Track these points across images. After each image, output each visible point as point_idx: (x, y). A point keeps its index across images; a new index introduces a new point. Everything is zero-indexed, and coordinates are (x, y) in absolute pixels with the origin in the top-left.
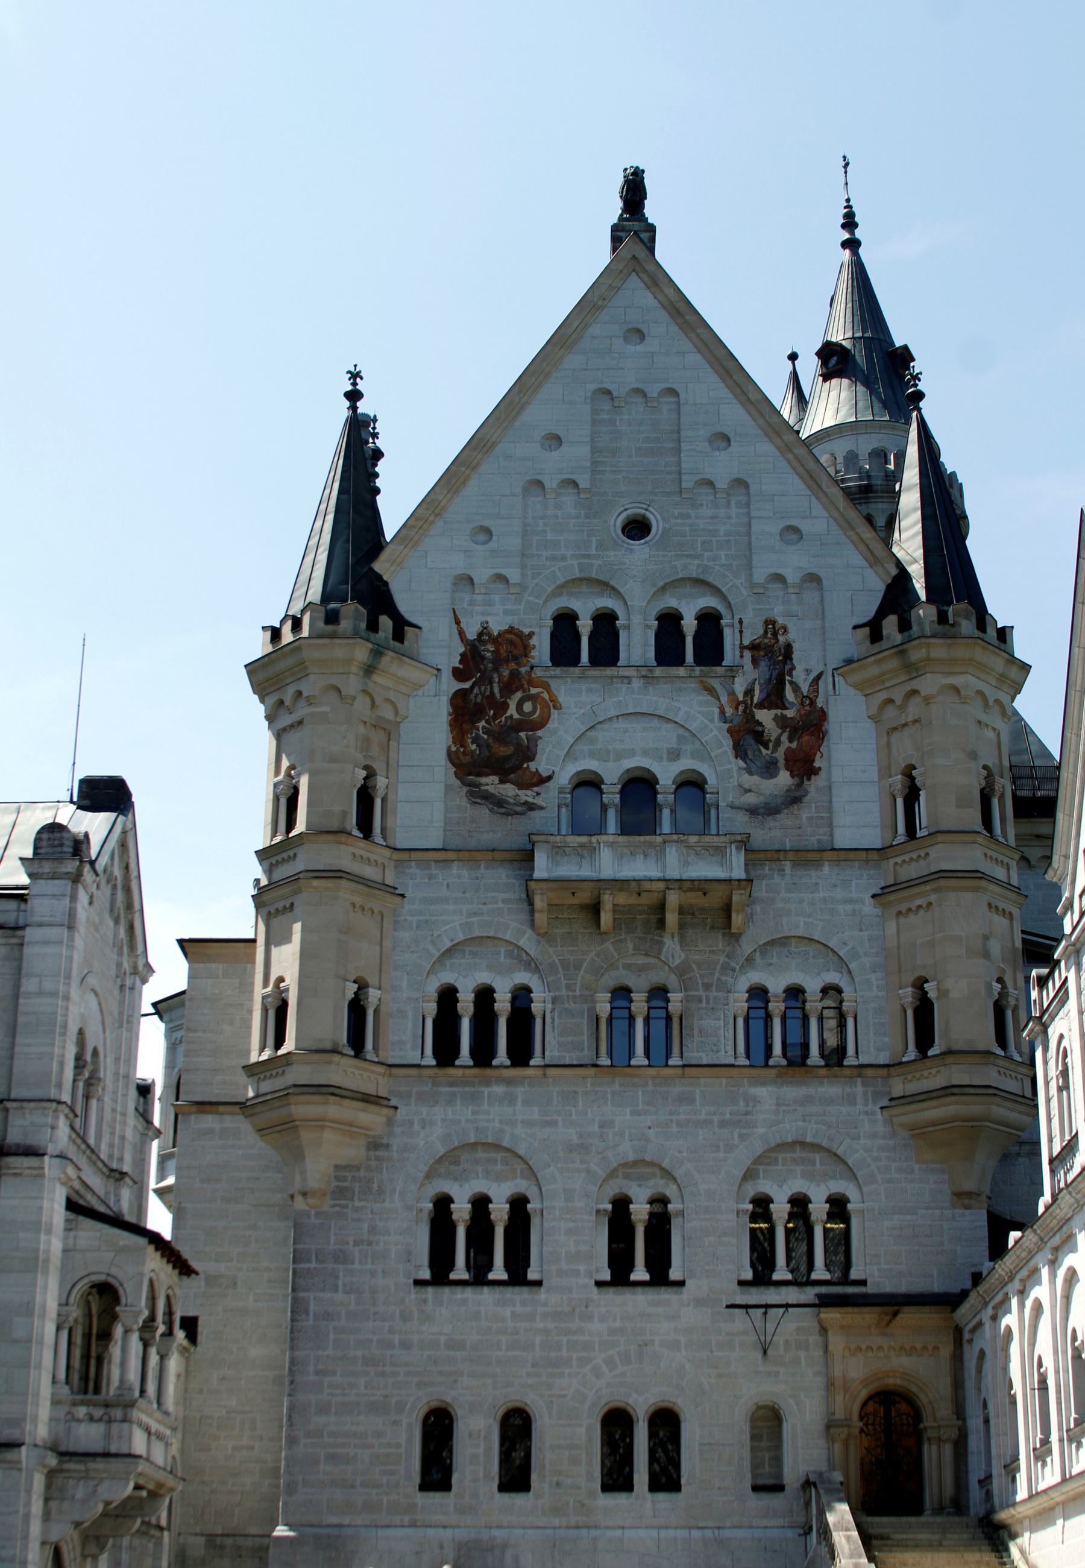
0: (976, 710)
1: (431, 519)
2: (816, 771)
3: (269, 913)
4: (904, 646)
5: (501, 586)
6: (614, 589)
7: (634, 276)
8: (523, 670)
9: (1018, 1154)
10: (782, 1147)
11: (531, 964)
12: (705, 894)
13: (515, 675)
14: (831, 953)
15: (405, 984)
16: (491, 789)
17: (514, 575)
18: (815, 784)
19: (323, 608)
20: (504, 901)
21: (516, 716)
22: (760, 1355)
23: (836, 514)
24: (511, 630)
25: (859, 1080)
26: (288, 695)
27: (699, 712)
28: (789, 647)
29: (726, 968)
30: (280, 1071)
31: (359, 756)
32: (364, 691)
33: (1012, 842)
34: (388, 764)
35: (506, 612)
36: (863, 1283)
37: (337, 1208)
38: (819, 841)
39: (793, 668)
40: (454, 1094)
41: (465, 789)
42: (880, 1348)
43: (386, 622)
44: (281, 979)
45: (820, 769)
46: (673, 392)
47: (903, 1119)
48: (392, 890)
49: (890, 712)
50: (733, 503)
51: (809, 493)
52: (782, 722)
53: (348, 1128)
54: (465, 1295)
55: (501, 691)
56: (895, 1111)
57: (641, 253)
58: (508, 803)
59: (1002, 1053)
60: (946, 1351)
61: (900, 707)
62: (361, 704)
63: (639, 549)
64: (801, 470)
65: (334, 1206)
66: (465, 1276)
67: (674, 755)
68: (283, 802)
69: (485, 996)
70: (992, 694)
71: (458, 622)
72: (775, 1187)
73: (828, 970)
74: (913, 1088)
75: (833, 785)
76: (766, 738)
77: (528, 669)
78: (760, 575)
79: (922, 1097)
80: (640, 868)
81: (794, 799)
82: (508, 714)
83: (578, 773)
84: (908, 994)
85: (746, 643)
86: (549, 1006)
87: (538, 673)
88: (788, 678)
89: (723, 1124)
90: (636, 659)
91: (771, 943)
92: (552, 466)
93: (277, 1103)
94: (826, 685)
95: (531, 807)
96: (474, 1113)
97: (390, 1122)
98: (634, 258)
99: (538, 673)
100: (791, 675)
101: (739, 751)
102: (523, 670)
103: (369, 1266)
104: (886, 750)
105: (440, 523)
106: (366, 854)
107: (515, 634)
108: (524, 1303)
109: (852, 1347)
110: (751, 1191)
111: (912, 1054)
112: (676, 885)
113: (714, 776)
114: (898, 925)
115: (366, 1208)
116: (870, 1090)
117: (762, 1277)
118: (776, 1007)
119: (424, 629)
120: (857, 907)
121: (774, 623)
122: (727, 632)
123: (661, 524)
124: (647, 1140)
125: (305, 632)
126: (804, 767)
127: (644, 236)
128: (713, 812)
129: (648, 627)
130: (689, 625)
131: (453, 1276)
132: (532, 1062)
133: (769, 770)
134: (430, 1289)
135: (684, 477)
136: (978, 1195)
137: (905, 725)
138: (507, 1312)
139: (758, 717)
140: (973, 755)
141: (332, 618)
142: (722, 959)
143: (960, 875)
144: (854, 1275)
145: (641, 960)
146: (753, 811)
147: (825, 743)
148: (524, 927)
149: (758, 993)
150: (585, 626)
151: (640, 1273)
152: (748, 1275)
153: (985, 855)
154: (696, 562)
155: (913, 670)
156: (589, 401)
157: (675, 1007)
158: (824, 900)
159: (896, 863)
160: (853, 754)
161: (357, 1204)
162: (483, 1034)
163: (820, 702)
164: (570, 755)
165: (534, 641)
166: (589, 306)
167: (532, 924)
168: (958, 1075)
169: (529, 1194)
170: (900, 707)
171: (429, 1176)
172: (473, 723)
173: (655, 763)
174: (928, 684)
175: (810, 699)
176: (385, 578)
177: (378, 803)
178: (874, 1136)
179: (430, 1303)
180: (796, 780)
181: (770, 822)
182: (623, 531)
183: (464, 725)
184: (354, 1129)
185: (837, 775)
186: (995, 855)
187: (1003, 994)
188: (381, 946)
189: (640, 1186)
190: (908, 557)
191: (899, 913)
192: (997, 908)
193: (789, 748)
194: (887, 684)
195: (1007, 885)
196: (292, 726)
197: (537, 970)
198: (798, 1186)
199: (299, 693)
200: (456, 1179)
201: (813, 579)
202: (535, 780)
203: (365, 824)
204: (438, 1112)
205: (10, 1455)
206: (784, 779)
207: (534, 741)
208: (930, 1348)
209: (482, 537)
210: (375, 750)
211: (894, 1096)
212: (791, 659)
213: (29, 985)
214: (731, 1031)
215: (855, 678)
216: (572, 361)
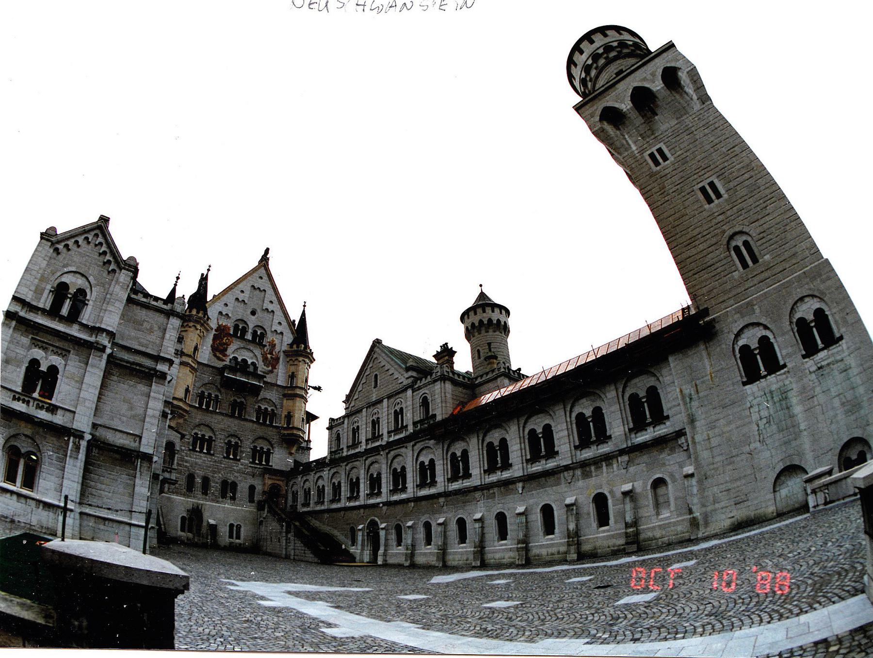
11: (220, 392)
18: (275, 371)
49: (291, 362)
67: (252, 358)
81: (271, 372)
92: (241, 297)
117: (253, 462)
126: (274, 367)
141: (198, 312)
149: (259, 407)
164: (233, 353)
166: (254, 270)
168: (295, 432)
174: (301, 359)
203: (194, 353)
206: (270, 368)
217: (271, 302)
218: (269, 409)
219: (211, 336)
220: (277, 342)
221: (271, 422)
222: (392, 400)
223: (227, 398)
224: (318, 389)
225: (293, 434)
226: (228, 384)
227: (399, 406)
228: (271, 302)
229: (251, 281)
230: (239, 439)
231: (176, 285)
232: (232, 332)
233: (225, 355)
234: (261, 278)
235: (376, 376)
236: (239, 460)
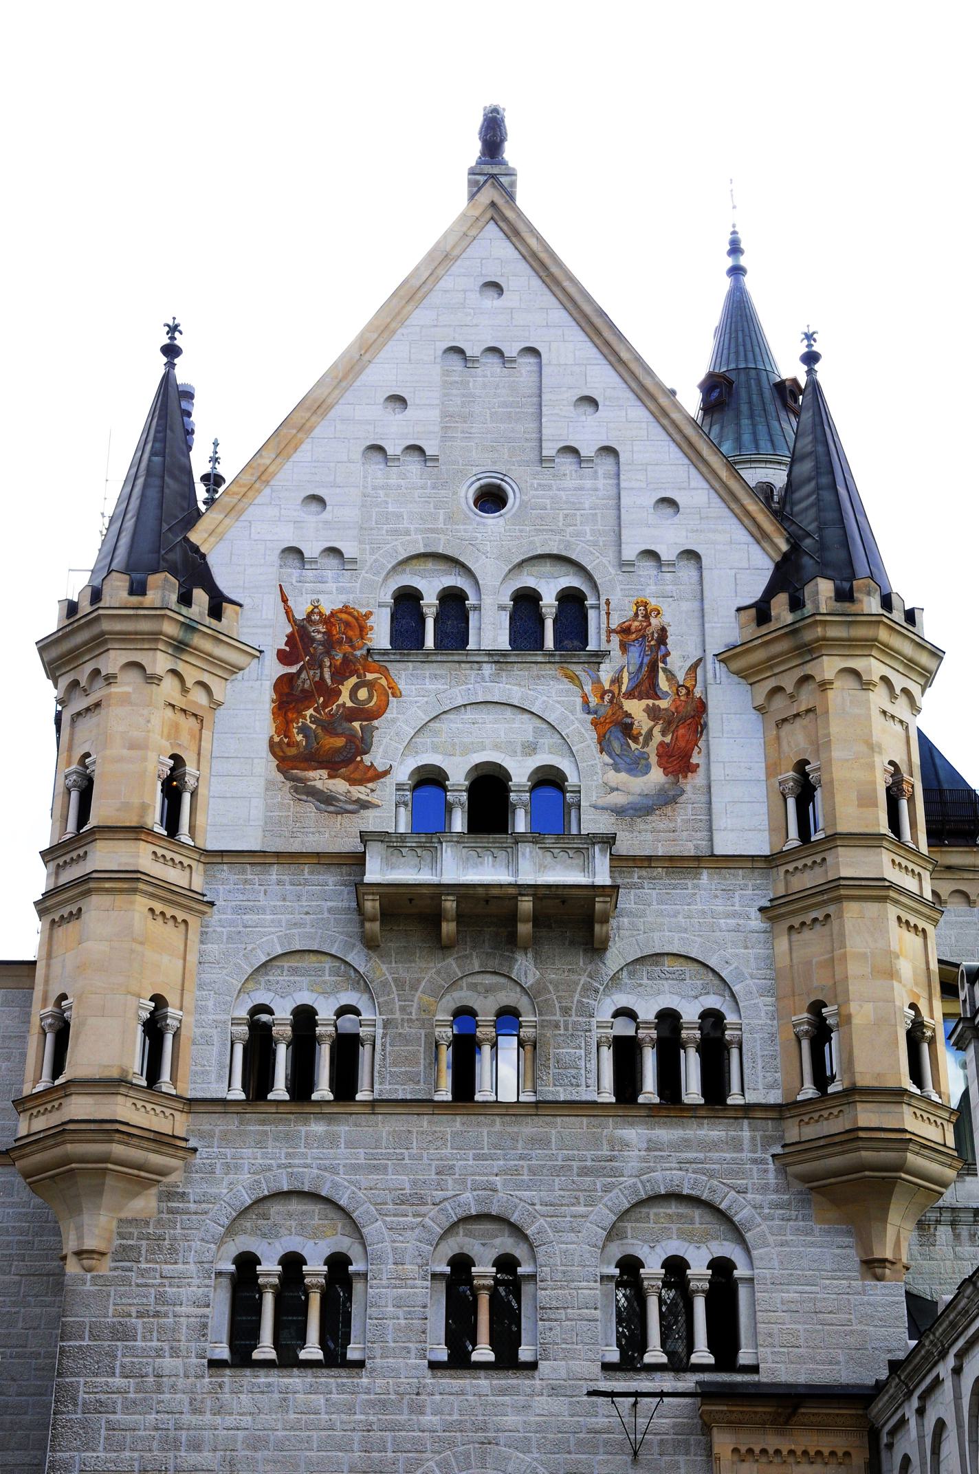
0: (879, 697)
1: (257, 485)
2: (693, 769)
3: (53, 921)
4: (797, 626)
5: (333, 562)
6: (463, 566)
7: (492, 225)
8: (358, 653)
9: (938, 1222)
10: (656, 1199)
11: (361, 982)
12: (563, 902)
13: (346, 659)
14: (711, 974)
15: (210, 1004)
16: (319, 784)
17: (349, 550)
18: (694, 782)
19: (127, 577)
20: (330, 910)
21: (349, 704)
22: (629, 1459)
23: (717, 486)
24: (346, 609)
25: (746, 1122)
26: (83, 675)
27: (558, 702)
28: (663, 630)
29: (587, 989)
30: (56, 1104)
31: (167, 744)
32: (174, 672)
33: (924, 848)
34: (199, 754)
35: (341, 591)
36: (754, 1369)
37: (119, 1272)
38: (696, 847)
39: (668, 654)
40: (266, 1133)
41: (289, 784)
42: (778, 1452)
43: (201, 597)
44: (63, 997)
45: (698, 765)
46: (533, 351)
47: (798, 1169)
49: (779, 702)
50: (600, 472)
51: (686, 461)
52: (653, 713)
53: (136, 1172)
54: (270, 1380)
55: (332, 676)
56: (789, 1160)
58: (338, 800)
59: (918, 1092)
60: (860, 1458)
61: (792, 696)
62: (170, 684)
63: (493, 522)
64: (678, 437)
65: (115, 1269)
66: (272, 1355)
67: (531, 749)
68: (74, 795)
70: (899, 682)
71: (285, 600)
72: (646, 1249)
73: (708, 993)
74: (810, 1132)
75: (713, 784)
76: (635, 732)
77: (364, 652)
78: (630, 553)
79: (822, 1143)
81: (666, 799)
82: (340, 702)
83: (420, 769)
85: (613, 627)
86: (380, 1032)
88: (661, 665)
89: (584, 1172)
90: (487, 645)
92: (396, 431)
93: (51, 1142)
94: (705, 672)
95: (365, 805)
96: (288, 1155)
97: (188, 1169)
98: (493, 204)
100: (664, 662)
102: (358, 653)
103: (155, 1344)
104: (773, 746)
105: (267, 491)
106: (169, 855)
107: (350, 614)
108: (341, 1389)
109: (743, 1449)
110: (617, 1251)
111: (809, 1091)
112: (530, 891)
113: (576, 773)
114: (790, 942)
115: (154, 1270)
116: (758, 1134)
119: (245, 607)
120: (741, 922)
121: (645, 604)
122: (592, 614)
123: (518, 495)
124: (496, 1191)
126: (679, 761)
127: (503, 179)
128: (574, 813)
129: (502, 608)
132: (359, 1097)
133: (637, 766)
134: (228, 1372)
135: (544, 445)
136: (893, 1263)
137: (797, 715)
138: (321, 1399)
139: (625, 708)
141: (138, 589)
142: (584, 979)
143: (863, 883)
144: (745, 1356)
145: (489, 980)
146: (619, 811)
147: (704, 737)
148: (352, 941)
151: (483, 1353)
152: (614, 1356)
153: (893, 861)
154: (557, 538)
156: (439, 360)
158: (704, 912)
159: (787, 871)
161: (143, 1266)
163: (698, 692)
165: (369, 623)
166: (442, 259)
168: (867, 1116)
169: (351, 1254)
170: (792, 696)
171: (231, 1230)
172: (300, 714)
173: (508, 758)
175: (687, 688)
176: (203, 550)
177: (187, 797)
178: (764, 1189)
179: (226, 1389)
180: (671, 778)
181: (640, 824)
182: (475, 504)
183: (290, 715)
184: (143, 1174)
185: (717, 772)
186: (904, 863)
188: (185, 959)
189: (483, 1245)
190: (801, 532)
191: (791, 928)
192: (907, 922)
193: (662, 744)
194: (776, 671)
195: (919, 898)
196: (88, 709)
197: (367, 989)
198: (674, 1247)
199: (96, 672)
200: (264, 1236)
201: (692, 555)
202: (371, 773)
204: (250, 1155)
206: (656, 776)
207: (368, 732)
208: (840, 1454)
209: (314, 507)
210: (185, 738)
211: (788, 1142)
212: (665, 644)
214: (594, 1062)
215: (738, 664)
216: (420, 317)
217: (591, 401)
218: (690, 1013)
219: (266, 696)
221: (715, 1084)
225: (853, 1137)
226: (409, 918)
228: (591, 401)
229: (433, 326)
232: (380, 635)
234: (495, 287)
236: (533, 1366)
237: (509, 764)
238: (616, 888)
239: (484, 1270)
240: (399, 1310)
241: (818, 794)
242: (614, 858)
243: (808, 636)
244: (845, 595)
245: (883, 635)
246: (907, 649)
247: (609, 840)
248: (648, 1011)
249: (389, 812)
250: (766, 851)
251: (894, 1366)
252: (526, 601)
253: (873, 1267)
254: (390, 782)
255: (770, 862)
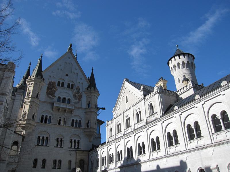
0: (96, 97)
10: (74, 135)
11: (52, 114)
13: (54, 86)
24: (54, 82)
28: (79, 89)
46: (72, 64)
48: (39, 104)
49: (88, 96)
52: (78, 95)
57: (71, 51)
60: (88, 156)
66: (41, 145)
67: (68, 96)
69: (47, 116)
80: (64, 106)
81: (78, 102)
84: (87, 122)
87: (56, 86)
91: (75, 115)
95: (54, 99)
99: (56, 86)
101: (74, 97)
110: (70, 139)
111: (87, 127)
118: (75, 121)
125: (34, 77)
126: (80, 100)
130: (71, 85)
131: (39, 145)
133: (76, 99)
140: (95, 101)
141: (37, 77)
142: (70, 116)
144: (80, 148)
146: (74, 103)
150: (61, 83)
155: (91, 93)
157: (65, 120)
160: (84, 99)
162: (44, 120)
167: (52, 110)
168: (92, 130)
174: (93, 94)
177: (38, 96)
187: (95, 123)
198: (75, 139)
201: (82, 83)
205: (4, 162)
206: (78, 100)
207: (55, 93)
213: (14, 106)
220: (80, 88)
221: (80, 127)
222: (135, 107)
223: (56, 116)
224: (104, 109)
225: (90, 131)
227: (139, 110)
228: (76, 69)
230: (63, 136)
231: (29, 68)
232: (57, 84)
233: (54, 96)
235: (127, 97)
236: (63, 147)
237: (66, 98)
238: (75, 109)
239: (60, 140)
240: (52, 142)
241: (90, 104)
242: (75, 107)
243: (91, 92)
244: (94, 89)
245: (97, 93)
246: (98, 94)
247: (74, 105)
248: (75, 119)
249: (56, 99)
250: (85, 108)
251: (91, 149)
252: (69, 84)
253: (90, 141)
254: (56, 97)
255: (86, 109)
